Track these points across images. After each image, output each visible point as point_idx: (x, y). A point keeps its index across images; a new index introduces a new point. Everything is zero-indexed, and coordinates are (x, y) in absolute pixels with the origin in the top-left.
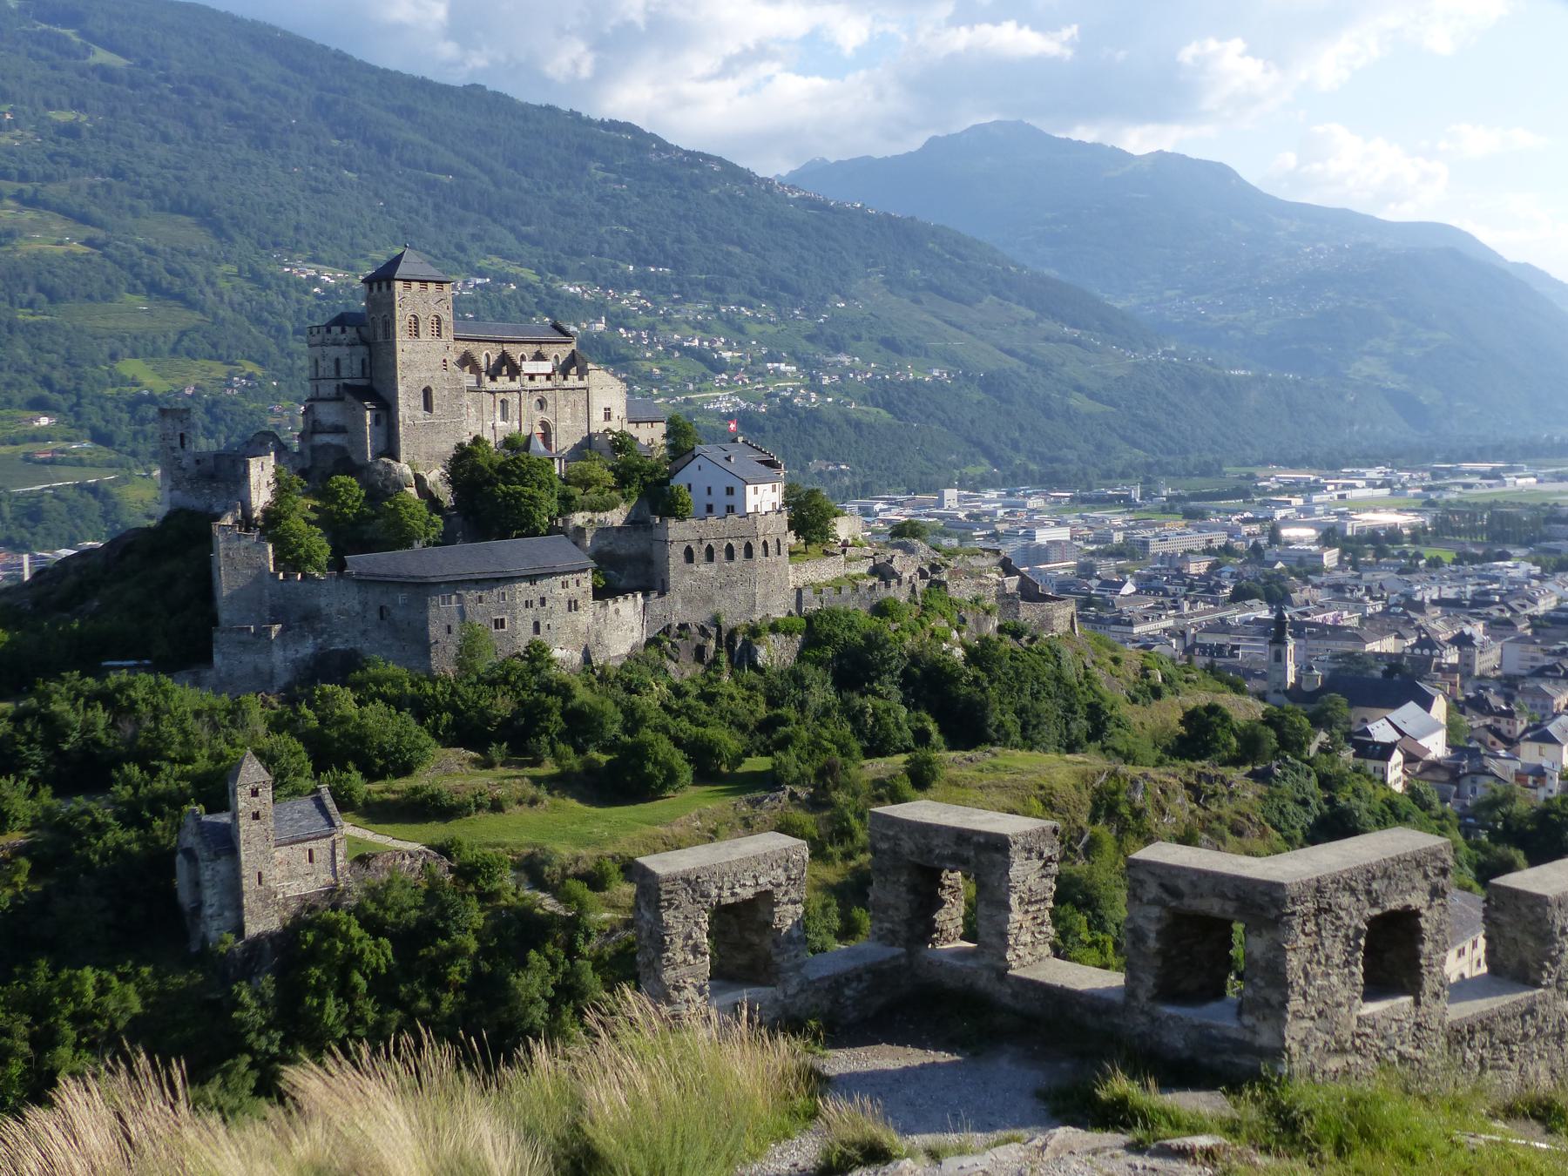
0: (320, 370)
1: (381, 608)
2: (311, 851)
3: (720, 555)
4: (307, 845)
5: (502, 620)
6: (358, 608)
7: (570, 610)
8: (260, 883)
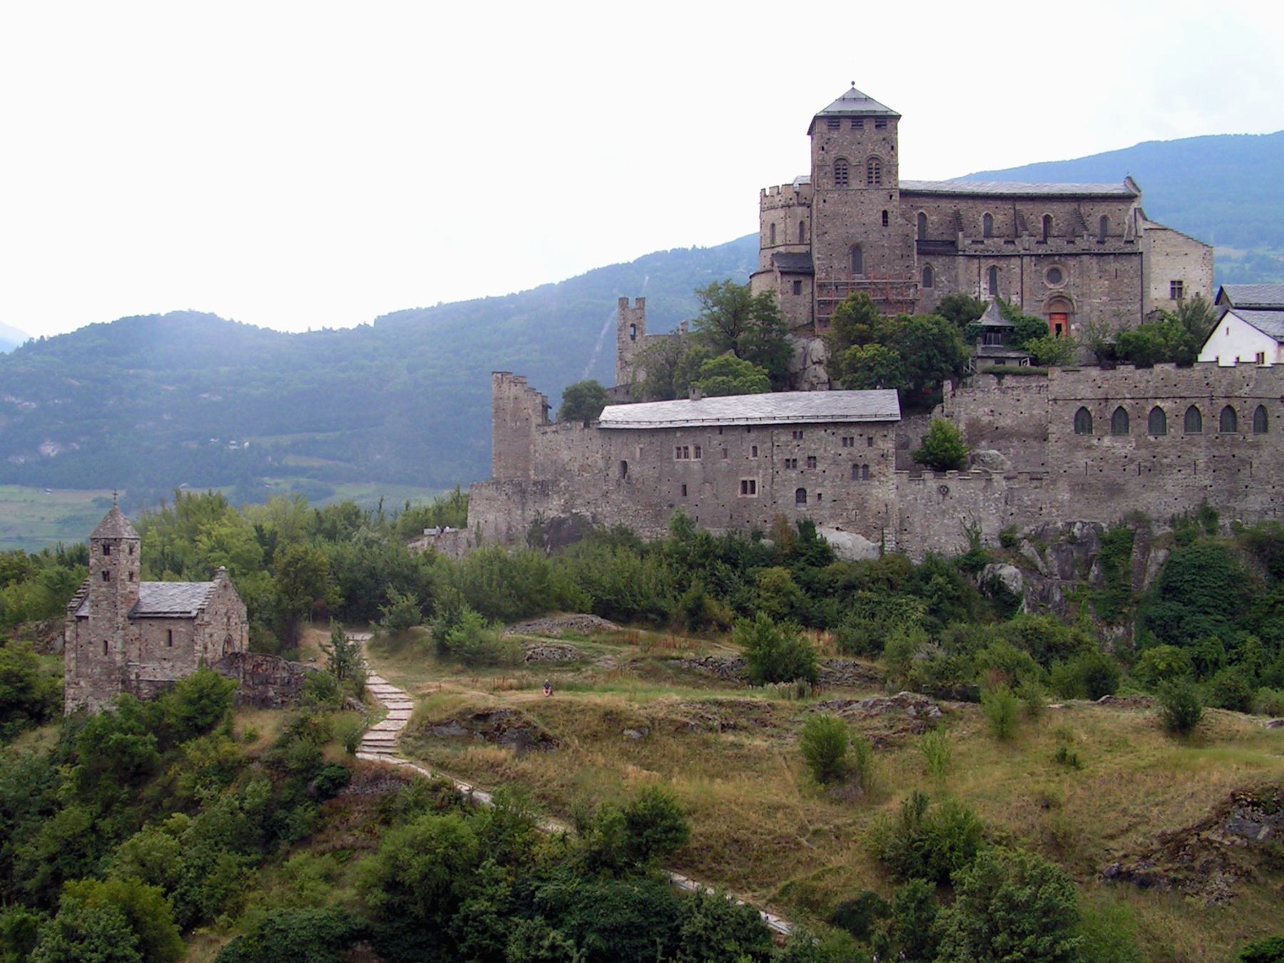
5: (753, 482)
6: (601, 463)
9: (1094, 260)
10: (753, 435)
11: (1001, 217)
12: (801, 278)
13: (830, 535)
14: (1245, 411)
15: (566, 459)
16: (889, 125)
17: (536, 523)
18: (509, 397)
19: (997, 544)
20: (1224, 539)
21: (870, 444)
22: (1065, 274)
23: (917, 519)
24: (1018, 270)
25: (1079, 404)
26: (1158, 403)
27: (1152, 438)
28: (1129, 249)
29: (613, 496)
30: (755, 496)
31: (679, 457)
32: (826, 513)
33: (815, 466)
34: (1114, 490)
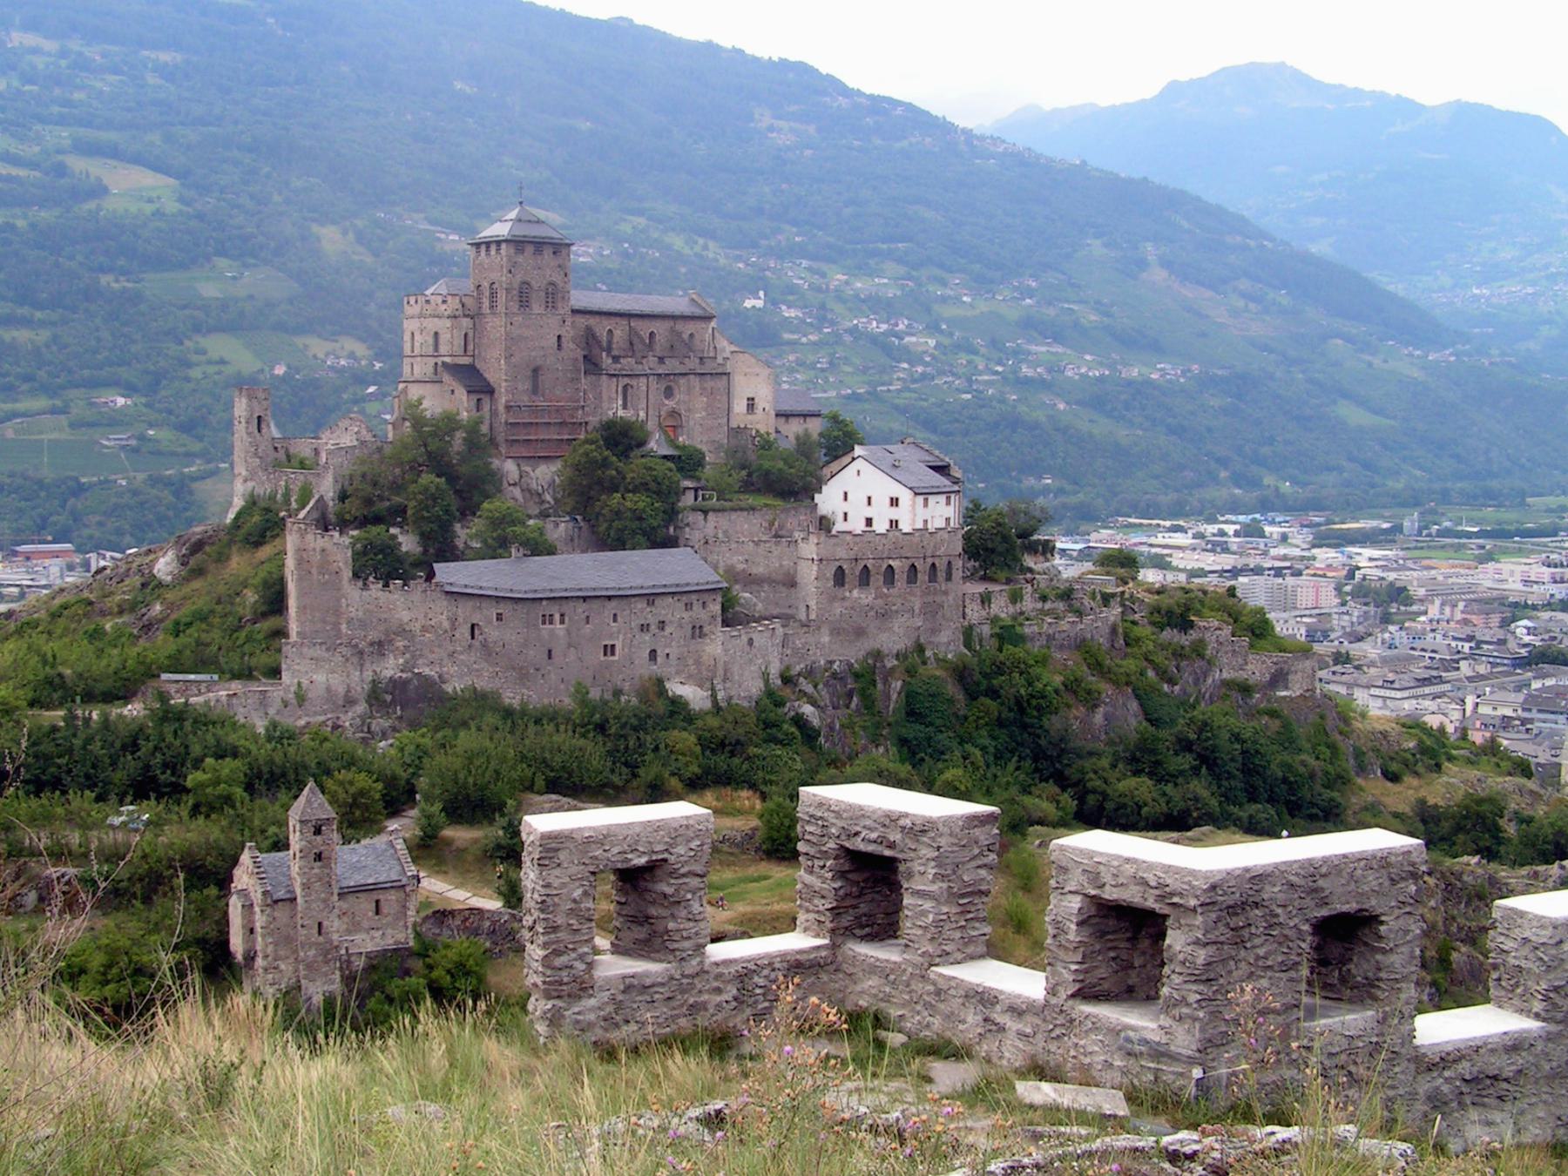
0: (417, 344)
1: (473, 626)
2: (377, 902)
3: (877, 580)
4: (375, 896)
5: (613, 646)
6: (446, 625)
7: (693, 637)
8: (320, 933)
9: (697, 379)
10: (614, 603)
11: (620, 332)
12: (482, 396)
13: (677, 688)
14: (941, 565)
15: (406, 620)
16: (564, 251)
17: (375, 683)
18: (314, 550)
19: (779, 682)
20: (933, 670)
21: (704, 607)
22: (676, 391)
23: (735, 669)
24: (644, 388)
25: (838, 564)
26: (891, 562)
27: (885, 590)
28: (720, 371)
29: (462, 657)
30: (616, 658)
31: (544, 623)
32: (673, 670)
33: (663, 629)
34: (860, 632)
